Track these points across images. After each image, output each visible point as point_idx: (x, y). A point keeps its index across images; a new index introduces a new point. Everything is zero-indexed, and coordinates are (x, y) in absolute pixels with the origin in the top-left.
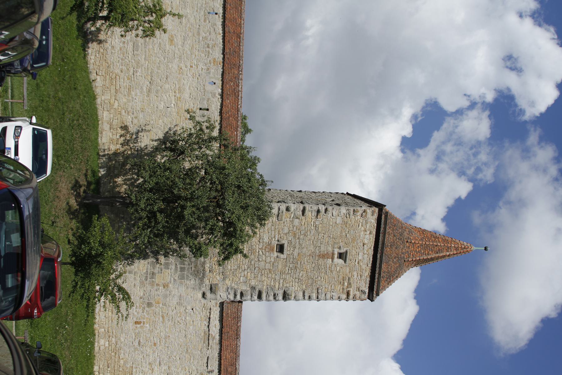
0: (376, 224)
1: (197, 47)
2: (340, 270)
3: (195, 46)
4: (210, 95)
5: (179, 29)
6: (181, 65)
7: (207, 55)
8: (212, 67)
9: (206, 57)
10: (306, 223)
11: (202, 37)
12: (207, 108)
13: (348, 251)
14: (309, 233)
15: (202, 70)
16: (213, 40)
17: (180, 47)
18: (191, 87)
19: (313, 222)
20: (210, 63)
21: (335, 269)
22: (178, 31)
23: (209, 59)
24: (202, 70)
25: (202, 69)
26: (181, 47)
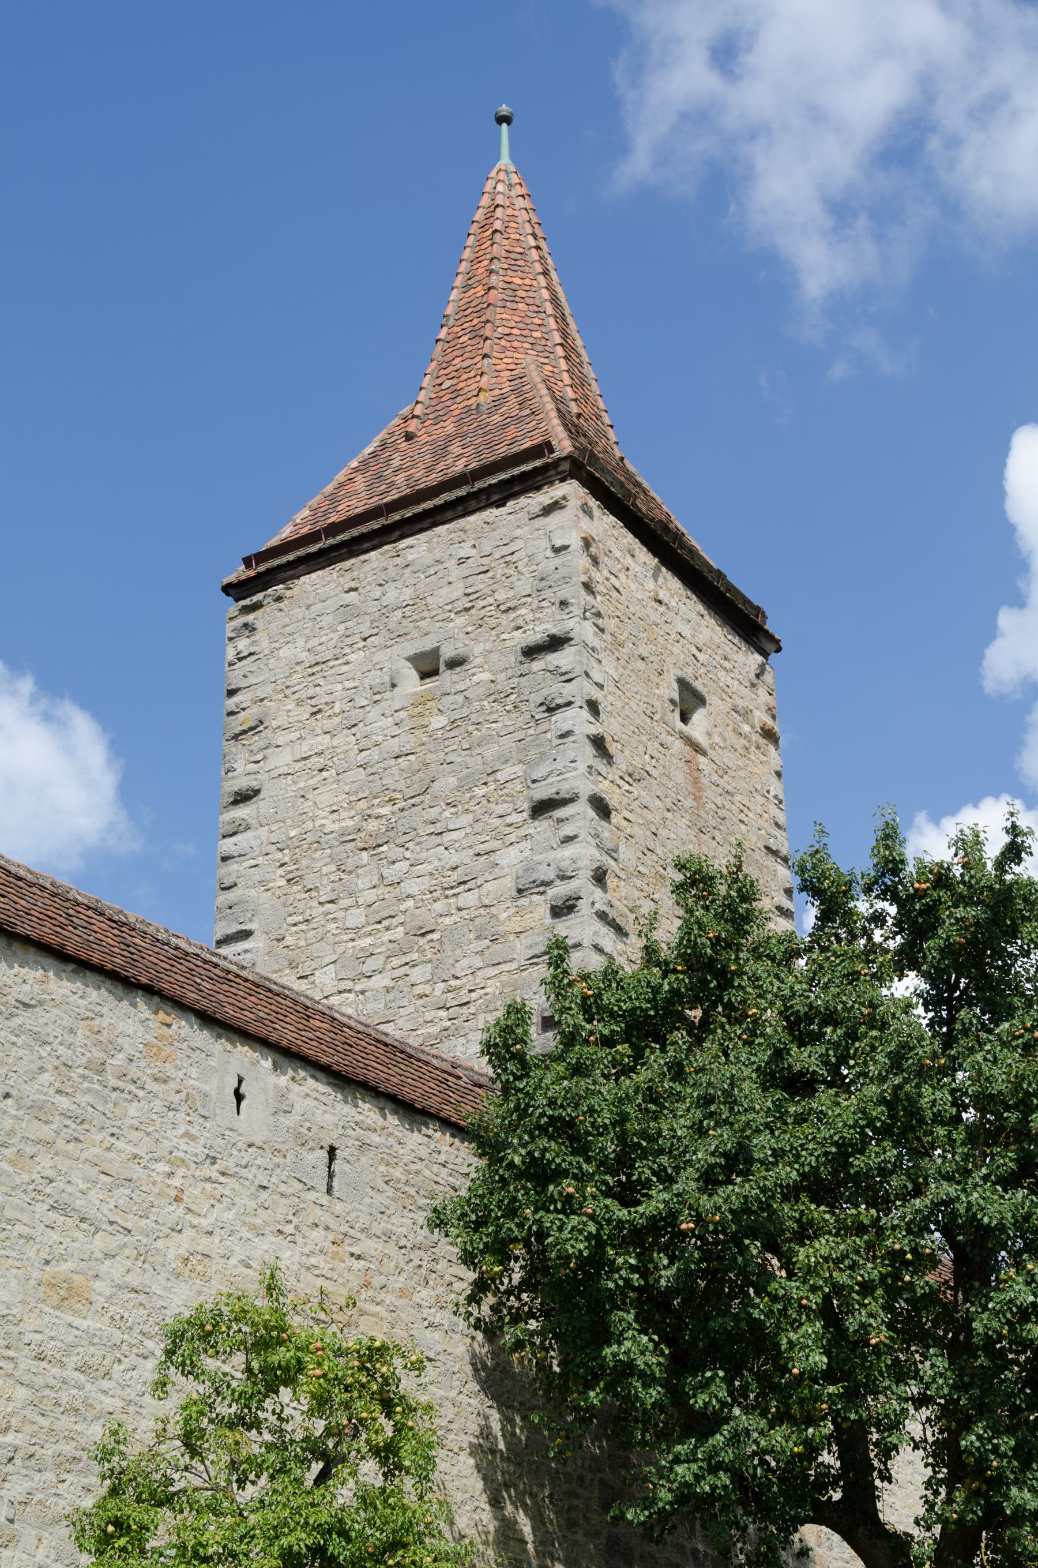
0: (611, 517)
1: (99, 1137)
2: (721, 735)
3: (97, 1150)
4: (286, 1121)
5: (19, 1228)
6: (171, 1255)
7: (132, 1088)
8: (181, 1074)
9: (140, 1093)
10: (628, 815)
11: (59, 1092)
12: (324, 1154)
13: (680, 673)
14: (650, 817)
15: (194, 1138)
16: (72, 1031)
17: (100, 1242)
18: (258, 1221)
19: (621, 782)
20: (165, 1082)
21: (720, 751)
22: (30, 1238)
23: (151, 1085)
24: (194, 1138)
25: (187, 1134)
26: (98, 1236)
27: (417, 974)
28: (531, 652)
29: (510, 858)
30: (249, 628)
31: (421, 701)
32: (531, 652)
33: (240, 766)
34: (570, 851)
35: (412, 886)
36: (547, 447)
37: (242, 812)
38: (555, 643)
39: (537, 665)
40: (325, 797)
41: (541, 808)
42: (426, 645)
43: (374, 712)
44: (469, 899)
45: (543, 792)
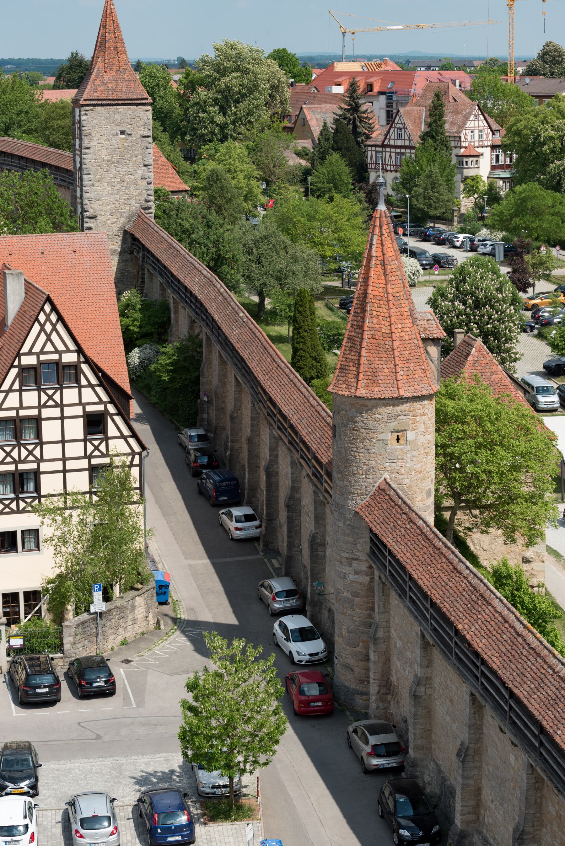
27: (123, 188)
28: (144, 137)
29: (140, 172)
30: (86, 115)
31: (122, 139)
32: (144, 137)
33: (86, 142)
34: (150, 174)
35: (122, 173)
36: (147, 99)
37: (87, 151)
38: (148, 137)
39: (144, 139)
40: (104, 152)
41: (145, 166)
42: (123, 129)
43: (113, 139)
44: (132, 177)
45: (146, 163)
